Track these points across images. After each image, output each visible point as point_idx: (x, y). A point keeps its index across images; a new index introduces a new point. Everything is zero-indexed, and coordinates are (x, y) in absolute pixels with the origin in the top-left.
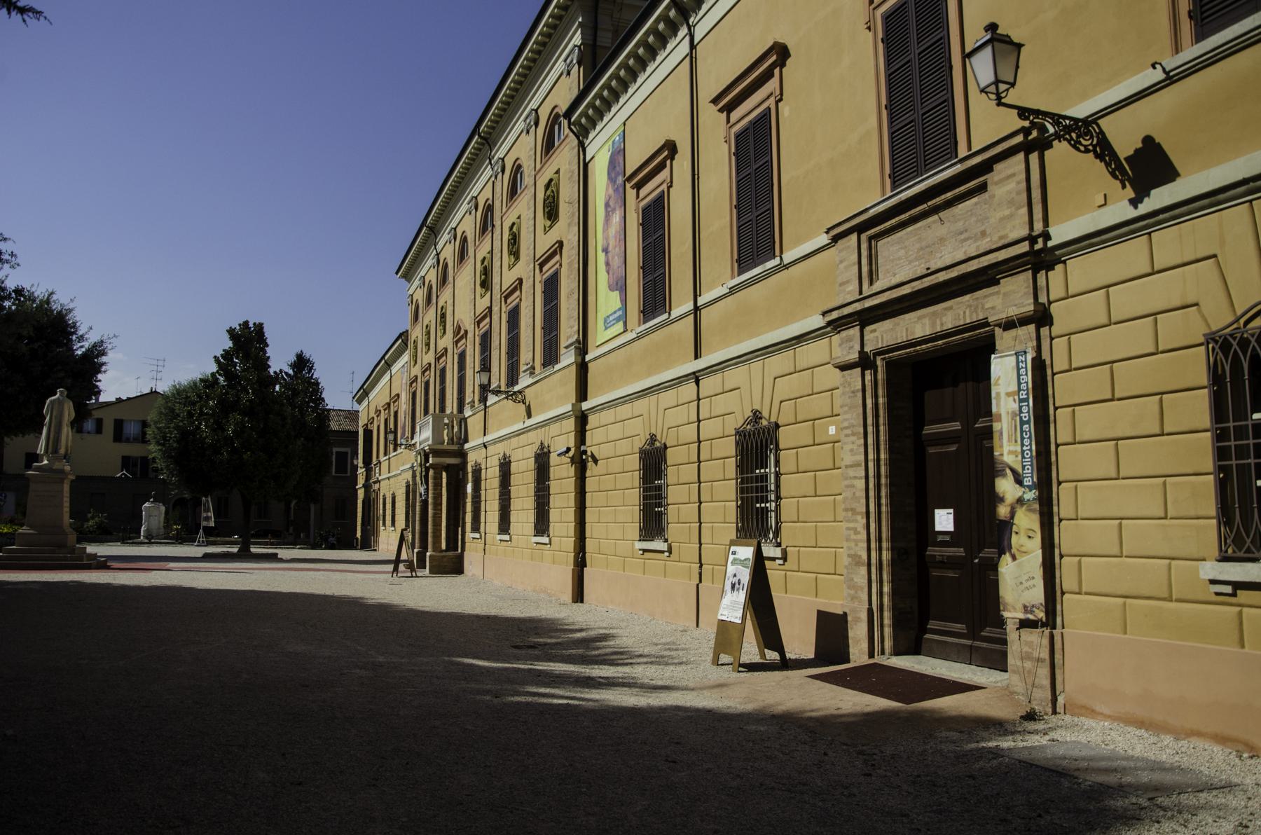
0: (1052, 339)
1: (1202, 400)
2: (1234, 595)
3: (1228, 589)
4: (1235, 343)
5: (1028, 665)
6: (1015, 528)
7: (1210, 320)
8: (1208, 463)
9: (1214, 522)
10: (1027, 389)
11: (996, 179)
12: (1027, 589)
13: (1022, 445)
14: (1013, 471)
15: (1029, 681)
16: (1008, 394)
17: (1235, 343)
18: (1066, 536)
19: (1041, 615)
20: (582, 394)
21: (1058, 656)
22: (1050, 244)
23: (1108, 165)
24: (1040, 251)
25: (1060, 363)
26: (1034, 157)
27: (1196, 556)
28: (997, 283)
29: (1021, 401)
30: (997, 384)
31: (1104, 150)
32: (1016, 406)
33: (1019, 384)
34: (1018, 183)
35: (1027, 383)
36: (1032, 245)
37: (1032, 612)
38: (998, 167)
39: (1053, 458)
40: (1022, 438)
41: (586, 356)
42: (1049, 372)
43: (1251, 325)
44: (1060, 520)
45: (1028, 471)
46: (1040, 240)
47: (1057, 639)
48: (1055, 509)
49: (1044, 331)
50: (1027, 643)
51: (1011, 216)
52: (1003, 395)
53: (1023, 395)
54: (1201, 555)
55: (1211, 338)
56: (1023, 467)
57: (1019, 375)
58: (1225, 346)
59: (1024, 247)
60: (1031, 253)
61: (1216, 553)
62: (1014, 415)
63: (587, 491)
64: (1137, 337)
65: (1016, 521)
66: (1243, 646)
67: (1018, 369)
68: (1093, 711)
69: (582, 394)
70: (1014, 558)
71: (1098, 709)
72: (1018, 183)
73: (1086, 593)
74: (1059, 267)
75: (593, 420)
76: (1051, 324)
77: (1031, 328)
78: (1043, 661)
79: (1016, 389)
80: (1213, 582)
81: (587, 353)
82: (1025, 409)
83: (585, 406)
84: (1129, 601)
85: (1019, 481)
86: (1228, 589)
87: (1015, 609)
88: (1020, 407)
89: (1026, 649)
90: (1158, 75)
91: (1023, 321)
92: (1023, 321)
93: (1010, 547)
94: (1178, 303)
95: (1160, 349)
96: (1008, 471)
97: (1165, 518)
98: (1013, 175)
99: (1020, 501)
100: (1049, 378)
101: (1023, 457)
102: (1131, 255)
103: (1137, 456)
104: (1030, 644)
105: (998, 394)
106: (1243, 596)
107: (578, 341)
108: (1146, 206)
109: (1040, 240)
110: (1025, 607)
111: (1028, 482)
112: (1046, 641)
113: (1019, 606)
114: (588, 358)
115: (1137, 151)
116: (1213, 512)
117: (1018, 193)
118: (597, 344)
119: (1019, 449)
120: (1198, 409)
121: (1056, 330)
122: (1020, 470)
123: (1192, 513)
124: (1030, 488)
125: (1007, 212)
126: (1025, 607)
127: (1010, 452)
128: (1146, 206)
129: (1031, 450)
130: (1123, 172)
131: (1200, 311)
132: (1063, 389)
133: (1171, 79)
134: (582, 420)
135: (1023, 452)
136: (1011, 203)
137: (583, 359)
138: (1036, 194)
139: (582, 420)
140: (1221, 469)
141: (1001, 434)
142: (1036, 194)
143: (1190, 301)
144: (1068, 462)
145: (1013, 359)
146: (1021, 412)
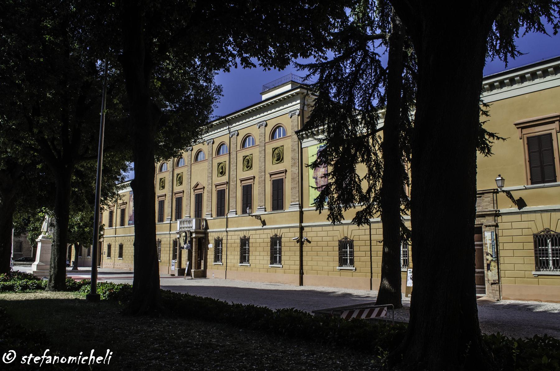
0: (498, 230)
1: (532, 244)
2: (538, 277)
3: (537, 276)
4: (539, 236)
5: (494, 291)
6: (491, 265)
7: (533, 231)
8: (533, 255)
9: (534, 265)
10: (494, 239)
11: (485, 196)
12: (494, 277)
13: (493, 250)
14: (491, 254)
15: (494, 295)
16: (489, 240)
17: (539, 236)
18: (501, 267)
19: (497, 282)
20: (301, 221)
21: (501, 289)
22: (500, 212)
23: (512, 200)
24: (498, 213)
25: (500, 234)
26: (495, 195)
27: (530, 270)
28: (485, 217)
29: (492, 241)
30: (486, 237)
31: (511, 197)
32: (491, 242)
33: (492, 238)
34: (491, 199)
35: (494, 238)
36: (496, 212)
37: (495, 281)
38: (486, 194)
39: (499, 252)
40: (493, 248)
41: (303, 209)
42: (498, 236)
43: (541, 234)
44: (500, 264)
45: (494, 254)
46: (498, 212)
47: (500, 286)
48: (499, 262)
49: (497, 228)
50: (493, 287)
51: (489, 205)
52: (488, 240)
53: (493, 240)
54: (532, 270)
55: (534, 235)
56: (493, 254)
57: (492, 236)
58: (537, 236)
59: (494, 212)
60: (496, 213)
61: (535, 270)
62: (491, 244)
63: (303, 250)
64: (519, 232)
65: (491, 264)
66: (539, 285)
67: (492, 235)
68: (509, 299)
69: (301, 221)
70: (491, 271)
71: (510, 298)
72: (491, 199)
73: (507, 277)
74: (500, 217)
75: (306, 229)
76: (498, 227)
77: (494, 227)
78: (497, 290)
79: (491, 239)
80: (534, 275)
81: (303, 208)
82: (493, 243)
83: (303, 225)
84: (516, 278)
85: (492, 256)
86: (537, 276)
87: (491, 281)
88: (492, 243)
89: (493, 288)
90: (524, 188)
91: (493, 226)
92: (493, 226)
93: (490, 269)
94: (527, 227)
95: (523, 235)
96: (489, 254)
97: (524, 264)
98: (490, 197)
99: (492, 260)
100: (498, 237)
101: (493, 252)
102: (518, 217)
103: (517, 253)
104: (494, 287)
105: (487, 240)
106: (539, 277)
107: (299, 204)
108: (521, 210)
109: (498, 212)
110: (494, 280)
111: (494, 257)
112: (498, 287)
113: (492, 280)
114: (303, 210)
115: (518, 199)
116: (534, 263)
117: (491, 201)
118: (309, 206)
119: (492, 250)
120: (532, 246)
121: (499, 228)
122: (492, 254)
123: (530, 263)
124: (494, 258)
125: (488, 204)
126: (494, 280)
127: (490, 251)
128: (521, 210)
129: (495, 251)
130: (515, 202)
131: (531, 229)
132: (500, 239)
133: (526, 189)
134: (302, 229)
135: (493, 251)
136: (489, 202)
137: (302, 210)
138: (495, 202)
139: (302, 229)
140: (536, 256)
141: (487, 247)
142: (495, 202)
143: (530, 227)
144: (502, 253)
145: (490, 233)
146: (492, 243)
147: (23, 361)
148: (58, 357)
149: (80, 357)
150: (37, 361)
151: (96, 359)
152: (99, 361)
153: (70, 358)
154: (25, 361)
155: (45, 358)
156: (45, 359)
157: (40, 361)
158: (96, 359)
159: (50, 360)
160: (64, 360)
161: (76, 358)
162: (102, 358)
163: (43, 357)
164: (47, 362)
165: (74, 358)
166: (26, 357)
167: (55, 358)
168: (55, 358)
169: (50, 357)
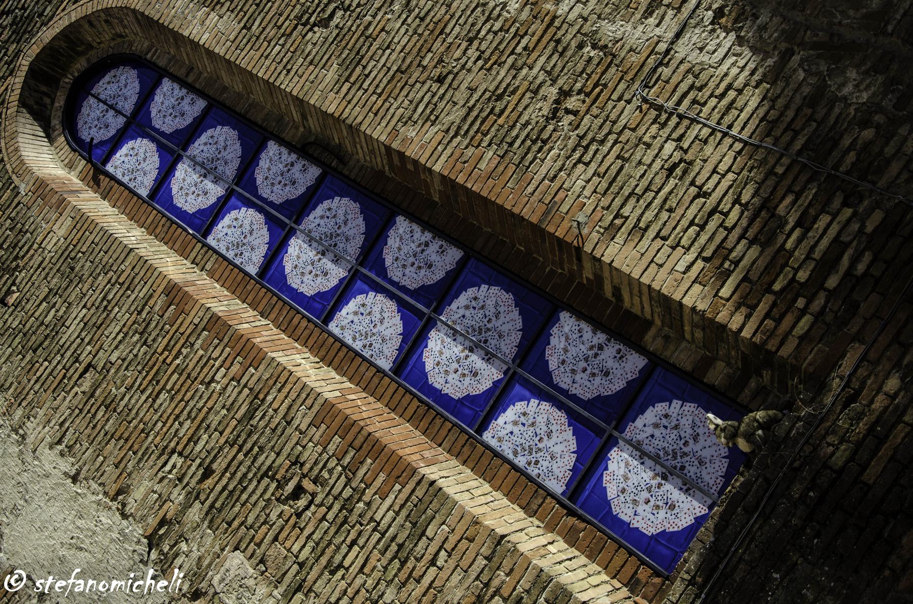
147: (38, 589)
148: (95, 582)
149: (130, 581)
150: (60, 588)
151: (156, 585)
152: (161, 588)
153: (114, 583)
154: (41, 587)
155: (74, 583)
156: (74, 585)
157: (64, 588)
158: (156, 585)
159: (82, 586)
160: (104, 586)
161: (123, 583)
162: (166, 583)
163: (71, 581)
164: (76, 590)
165: (120, 583)
166: (42, 581)
167: (90, 582)
168: (90, 582)
169: (81, 582)
